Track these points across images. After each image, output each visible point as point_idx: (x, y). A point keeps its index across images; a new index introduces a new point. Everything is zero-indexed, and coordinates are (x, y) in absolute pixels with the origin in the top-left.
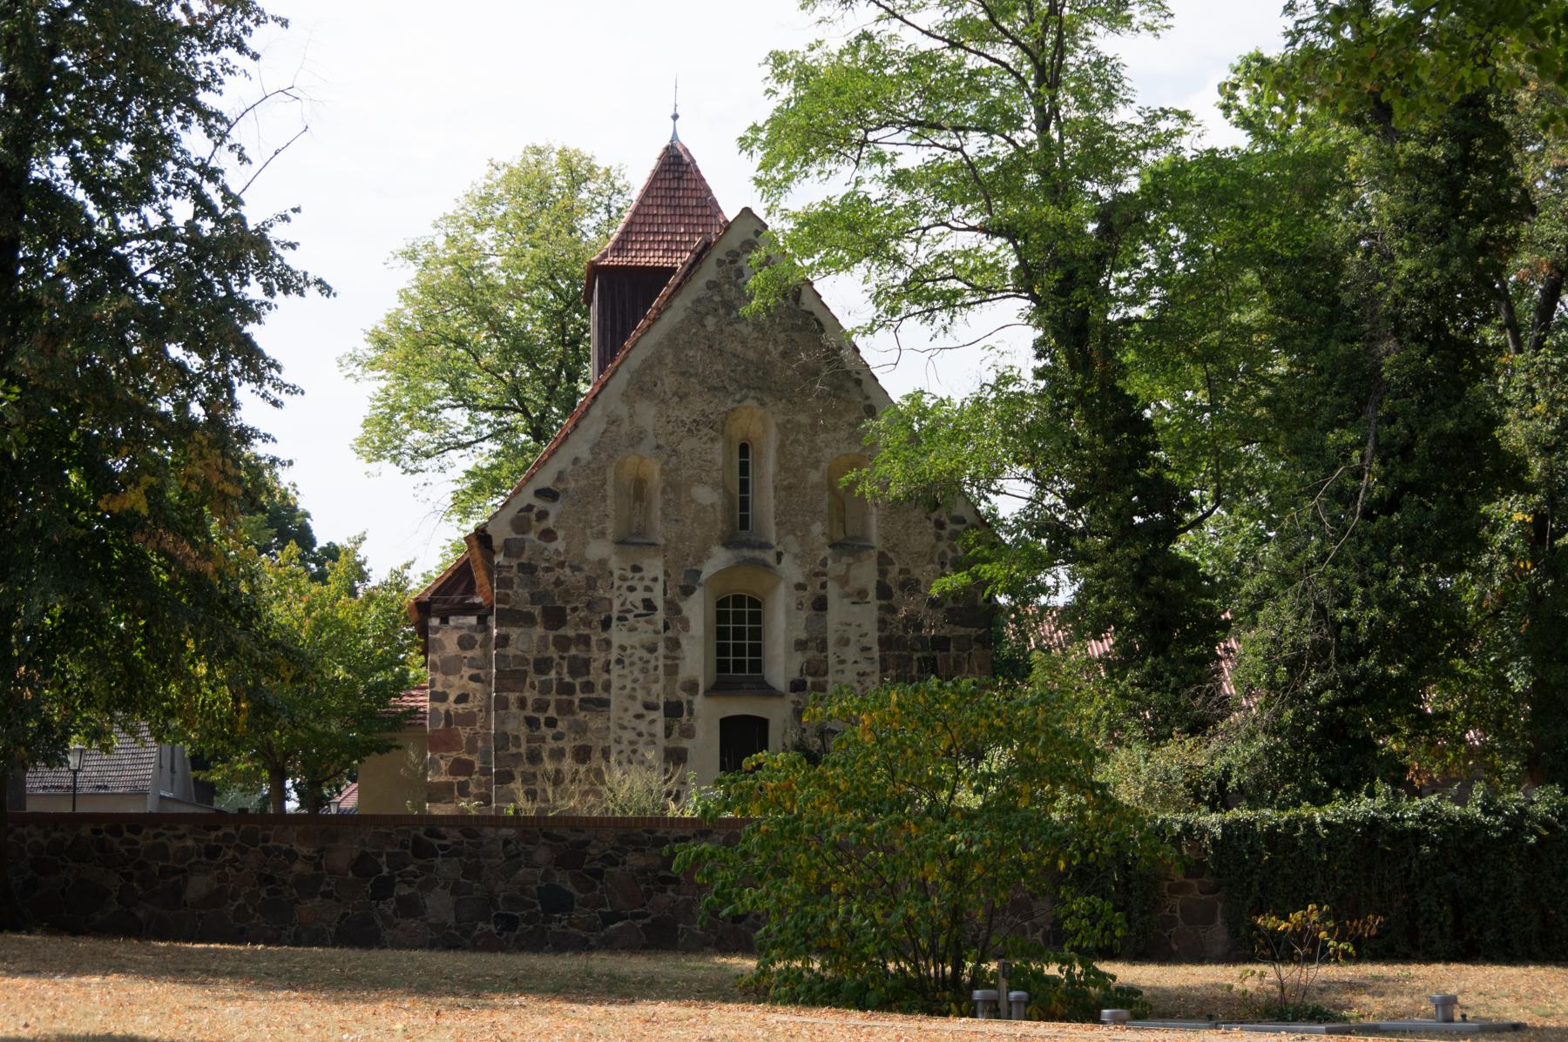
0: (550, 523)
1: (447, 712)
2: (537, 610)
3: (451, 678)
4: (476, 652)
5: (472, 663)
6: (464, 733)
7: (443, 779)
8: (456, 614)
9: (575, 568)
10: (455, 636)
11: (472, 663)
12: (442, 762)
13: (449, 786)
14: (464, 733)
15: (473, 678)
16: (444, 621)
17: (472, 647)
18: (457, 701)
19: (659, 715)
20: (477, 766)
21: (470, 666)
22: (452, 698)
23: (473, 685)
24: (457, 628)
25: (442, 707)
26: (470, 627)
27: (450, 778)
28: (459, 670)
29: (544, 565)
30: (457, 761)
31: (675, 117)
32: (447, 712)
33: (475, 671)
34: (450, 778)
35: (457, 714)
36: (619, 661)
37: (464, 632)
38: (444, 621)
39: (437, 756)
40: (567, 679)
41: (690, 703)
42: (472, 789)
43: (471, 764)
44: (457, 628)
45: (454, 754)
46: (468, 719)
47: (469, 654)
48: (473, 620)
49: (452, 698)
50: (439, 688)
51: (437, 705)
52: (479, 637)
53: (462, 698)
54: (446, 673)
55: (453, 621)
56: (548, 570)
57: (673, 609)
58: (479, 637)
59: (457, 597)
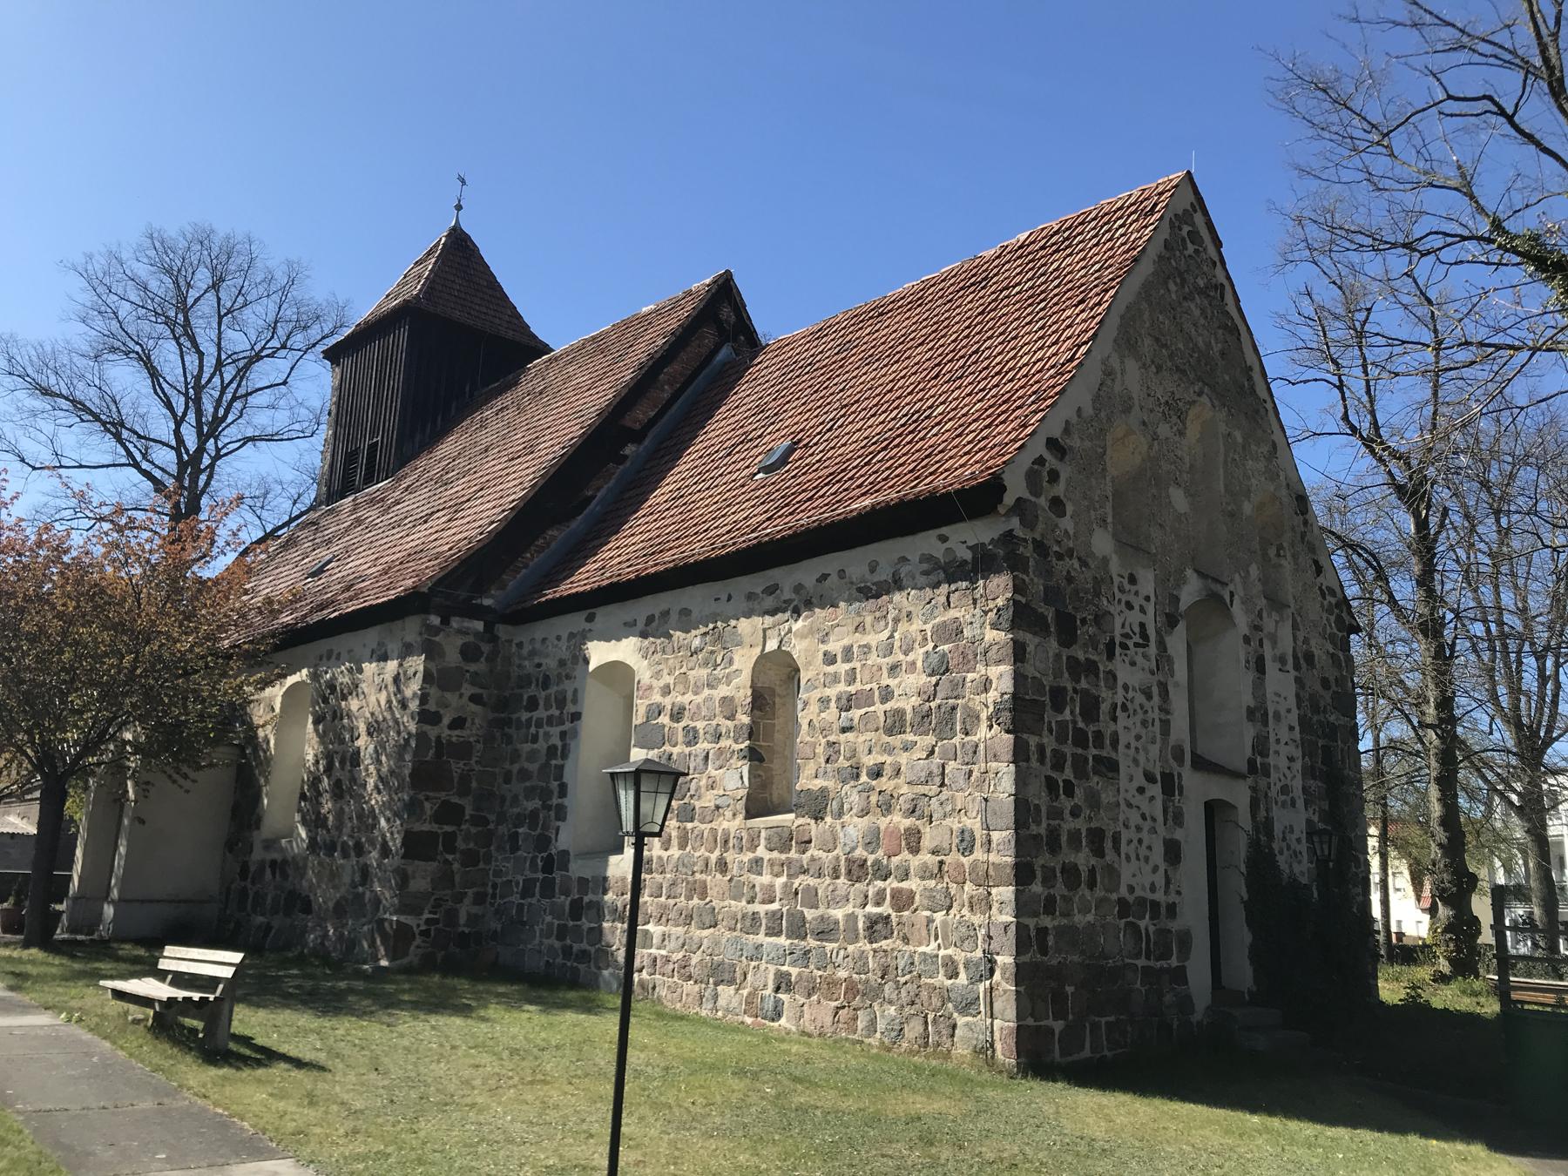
0: (1059, 489)
1: (438, 738)
2: (1050, 615)
3: (448, 695)
4: (480, 666)
5: (475, 679)
6: (457, 767)
7: (426, 827)
8: (461, 615)
9: (1084, 563)
10: (459, 641)
11: (475, 679)
12: (427, 805)
13: (432, 835)
14: (457, 767)
15: (475, 699)
16: (445, 621)
17: (475, 659)
18: (452, 726)
19: (1156, 790)
20: (469, 811)
21: (473, 684)
22: (446, 721)
23: (473, 707)
24: (460, 632)
25: (432, 732)
26: (477, 634)
27: (435, 827)
28: (459, 687)
29: (1056, 548)
30: (445, 804)
31: (459, 207)
32: (438, 738)
33: (477, 690)
34: (435, 827)
35: (450, 742)
36: (1124, 708)
37: (470, 639)
38: (445, 621)
39: (421, 797)
40: (1081, 725)
41: (1180, 775)
42: (460, 844)
43: (461, 809)
44: (460, 632)
45: (443, 795)
46: (463, 751)
47: (473, 667)
48: (479, 626)
49: (446, 721)
50: (431, 706)
51: (427, 728)
52: (486, 648)
53: (458, 723)
54: (443, 688)
55: (455, 623)
56: (1060, 557)
57: (1161, 645)
58: (486, 648)
59: (463, 594)
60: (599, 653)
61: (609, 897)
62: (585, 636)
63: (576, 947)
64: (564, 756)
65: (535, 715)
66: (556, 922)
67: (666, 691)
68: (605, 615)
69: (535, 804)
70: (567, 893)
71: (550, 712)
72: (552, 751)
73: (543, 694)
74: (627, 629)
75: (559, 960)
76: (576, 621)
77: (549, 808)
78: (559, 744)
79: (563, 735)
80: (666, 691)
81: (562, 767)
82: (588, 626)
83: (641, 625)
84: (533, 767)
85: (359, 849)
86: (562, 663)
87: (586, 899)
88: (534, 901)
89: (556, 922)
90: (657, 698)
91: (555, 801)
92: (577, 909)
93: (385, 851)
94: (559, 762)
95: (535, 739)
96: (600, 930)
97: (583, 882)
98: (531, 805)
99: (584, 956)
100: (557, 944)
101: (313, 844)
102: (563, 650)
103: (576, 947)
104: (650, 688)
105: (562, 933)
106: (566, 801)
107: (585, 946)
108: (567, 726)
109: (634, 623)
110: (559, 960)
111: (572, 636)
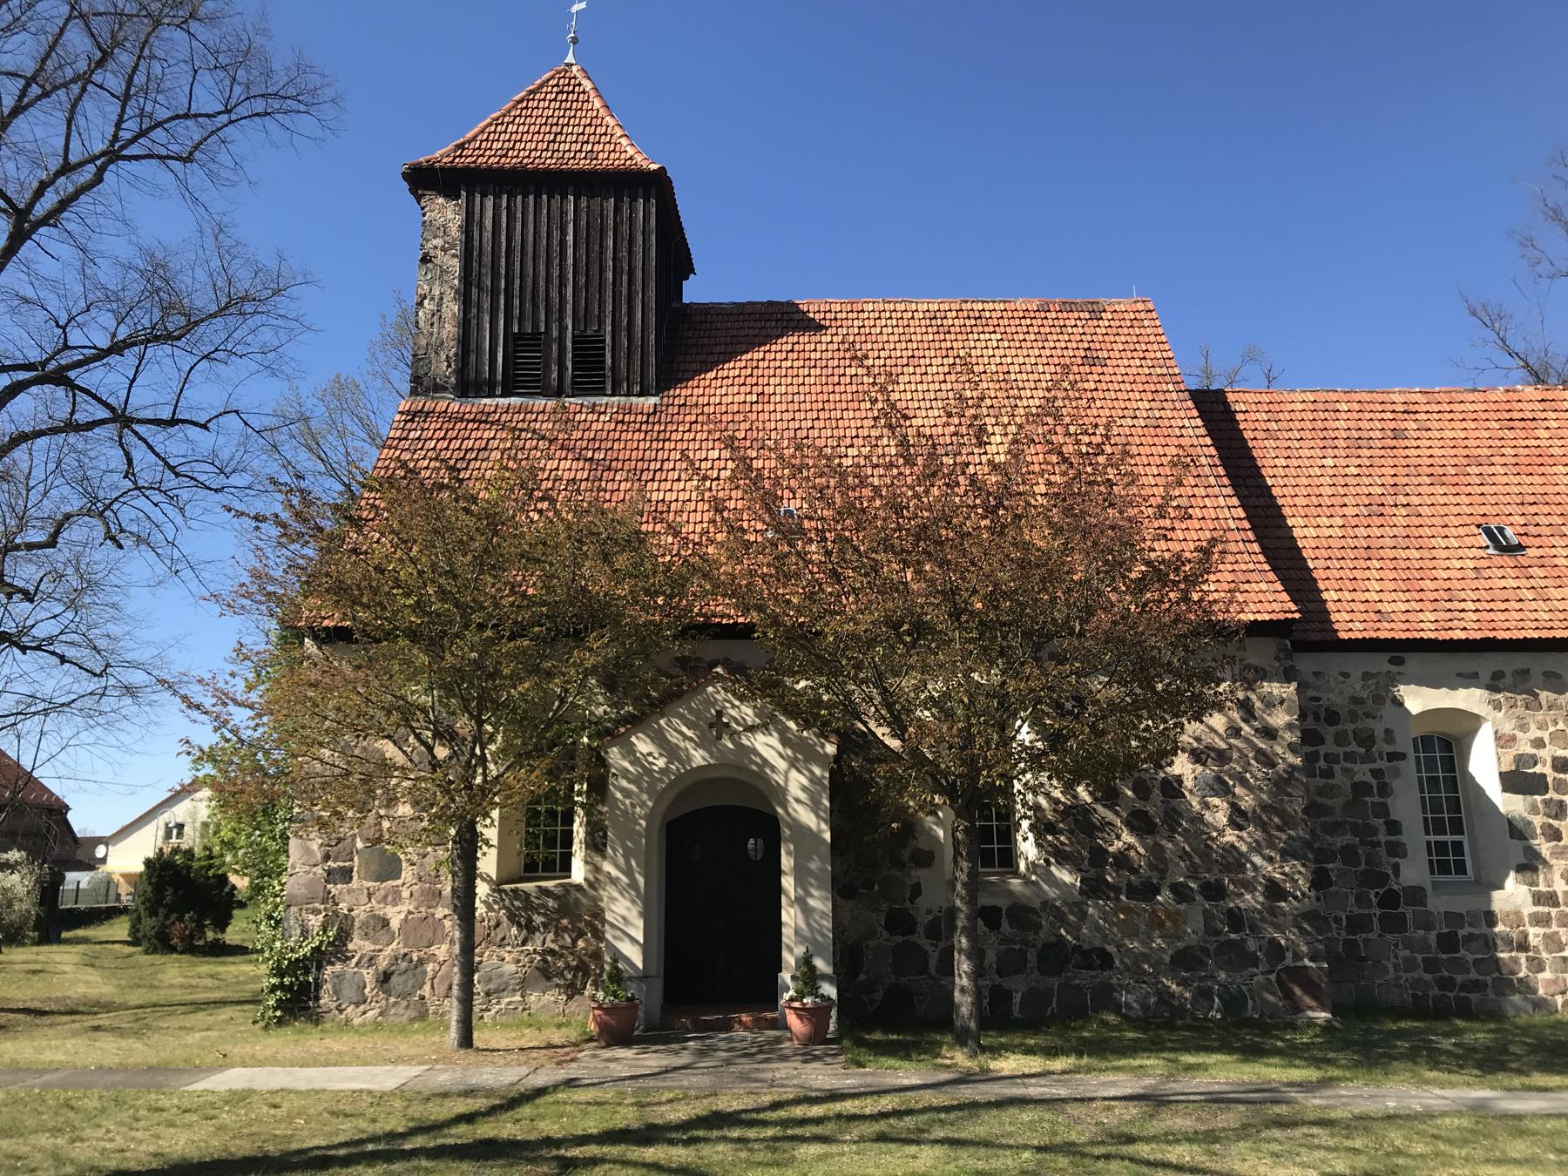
60: (1417, 700)
61: (1499, 928)
62: (1394, 680)
63: (1459, 979)
64: (1384, 790)
65: (1322, 750)
66: (1419, 957)
67: (1539, 743)
68: (1414, 661)
69: (1349, 838)
70: (1428, 927)
71: (1348, 749)
72: (1361, 789)
73: (1332, 729)
74: (1468, 679)
75: (1435, 992)
76: (1380, 663)
77: (1379, 844)
78: (1374, 783)
79: (1377, 773)
80: (1539, 743)
81: (1385, 805)
82: (1395, 669)
83: (1486, 677)
84: (1336, 803)
85: (1214, 892)
86: (1356, 701)
87: (1462, 933)
88: (1370, 936)
89: (1419, 957)
90: (1530, 750)
91: (1382, 837)
92: (1448, 942)
93: (1275, 891)
94: (1377, 799)
95: (1328, 774)
96: (1497, 961)
97: (1454, 918)
98: (1339, 841)
99: (1478, 986)
100: (1428, 977)
101: (1093, 887)
102: (1356, 686)
103: (1459, 979)
104: (1513, 739)
105: (1431, 965)
106: (1403, 839)
107: (1473, 975)
108: (1382, 764)
109: (1476, 675)
110: (1435, 992)
111: (1366, 676)
